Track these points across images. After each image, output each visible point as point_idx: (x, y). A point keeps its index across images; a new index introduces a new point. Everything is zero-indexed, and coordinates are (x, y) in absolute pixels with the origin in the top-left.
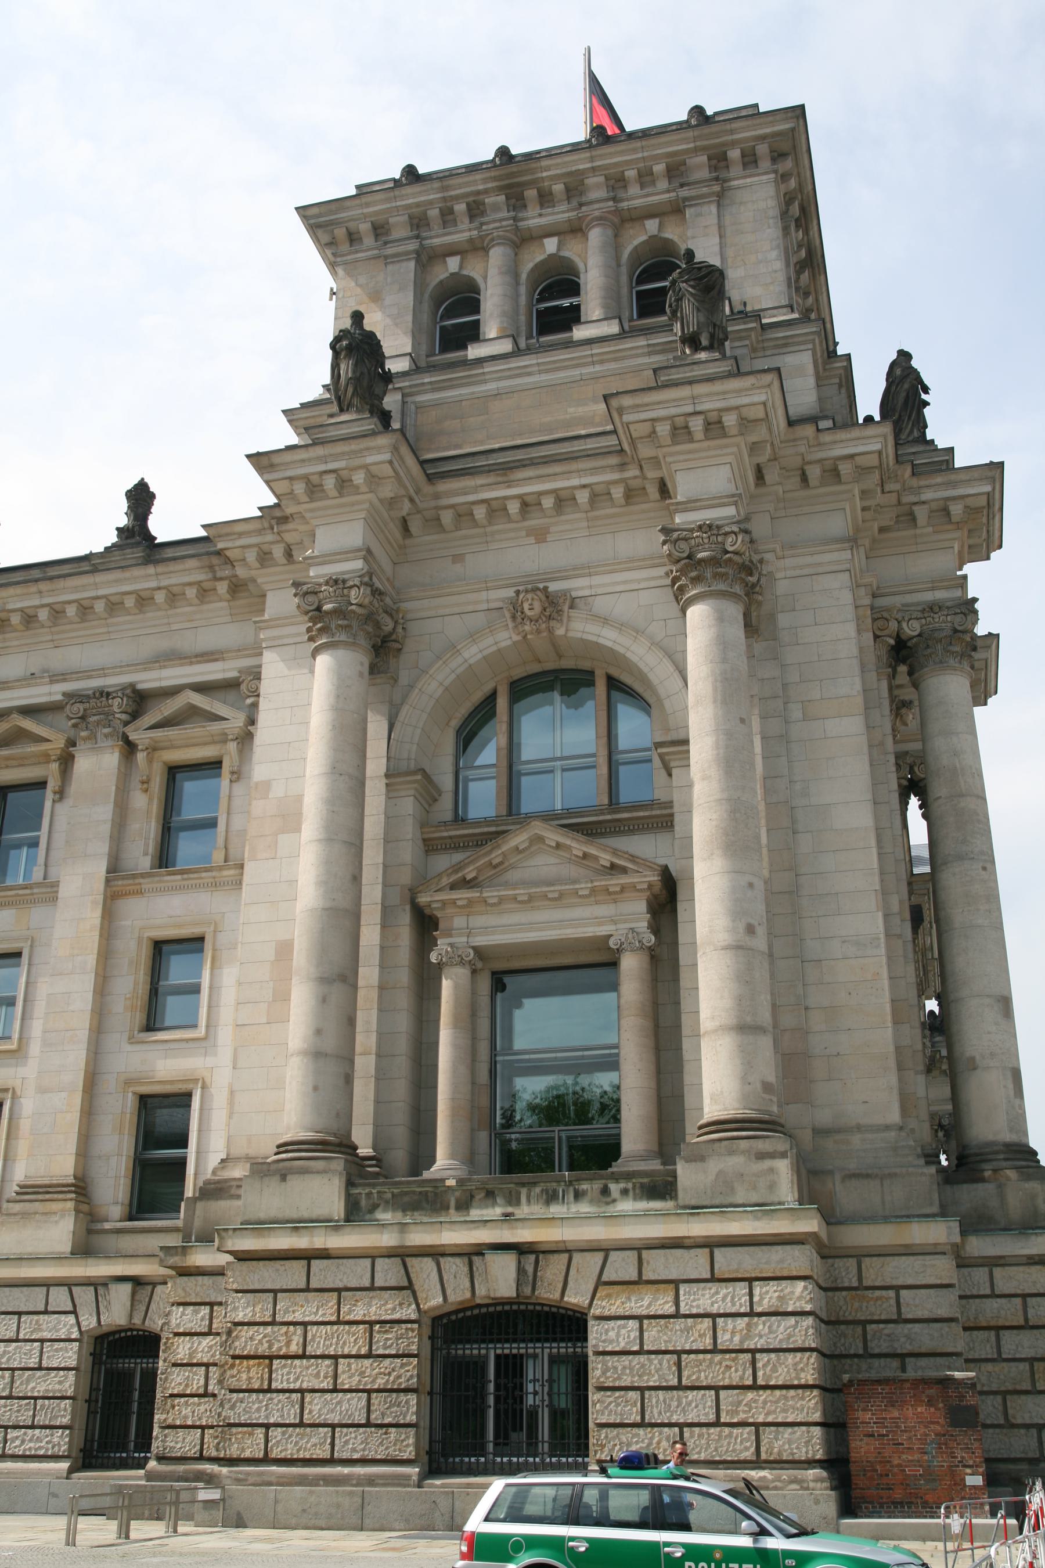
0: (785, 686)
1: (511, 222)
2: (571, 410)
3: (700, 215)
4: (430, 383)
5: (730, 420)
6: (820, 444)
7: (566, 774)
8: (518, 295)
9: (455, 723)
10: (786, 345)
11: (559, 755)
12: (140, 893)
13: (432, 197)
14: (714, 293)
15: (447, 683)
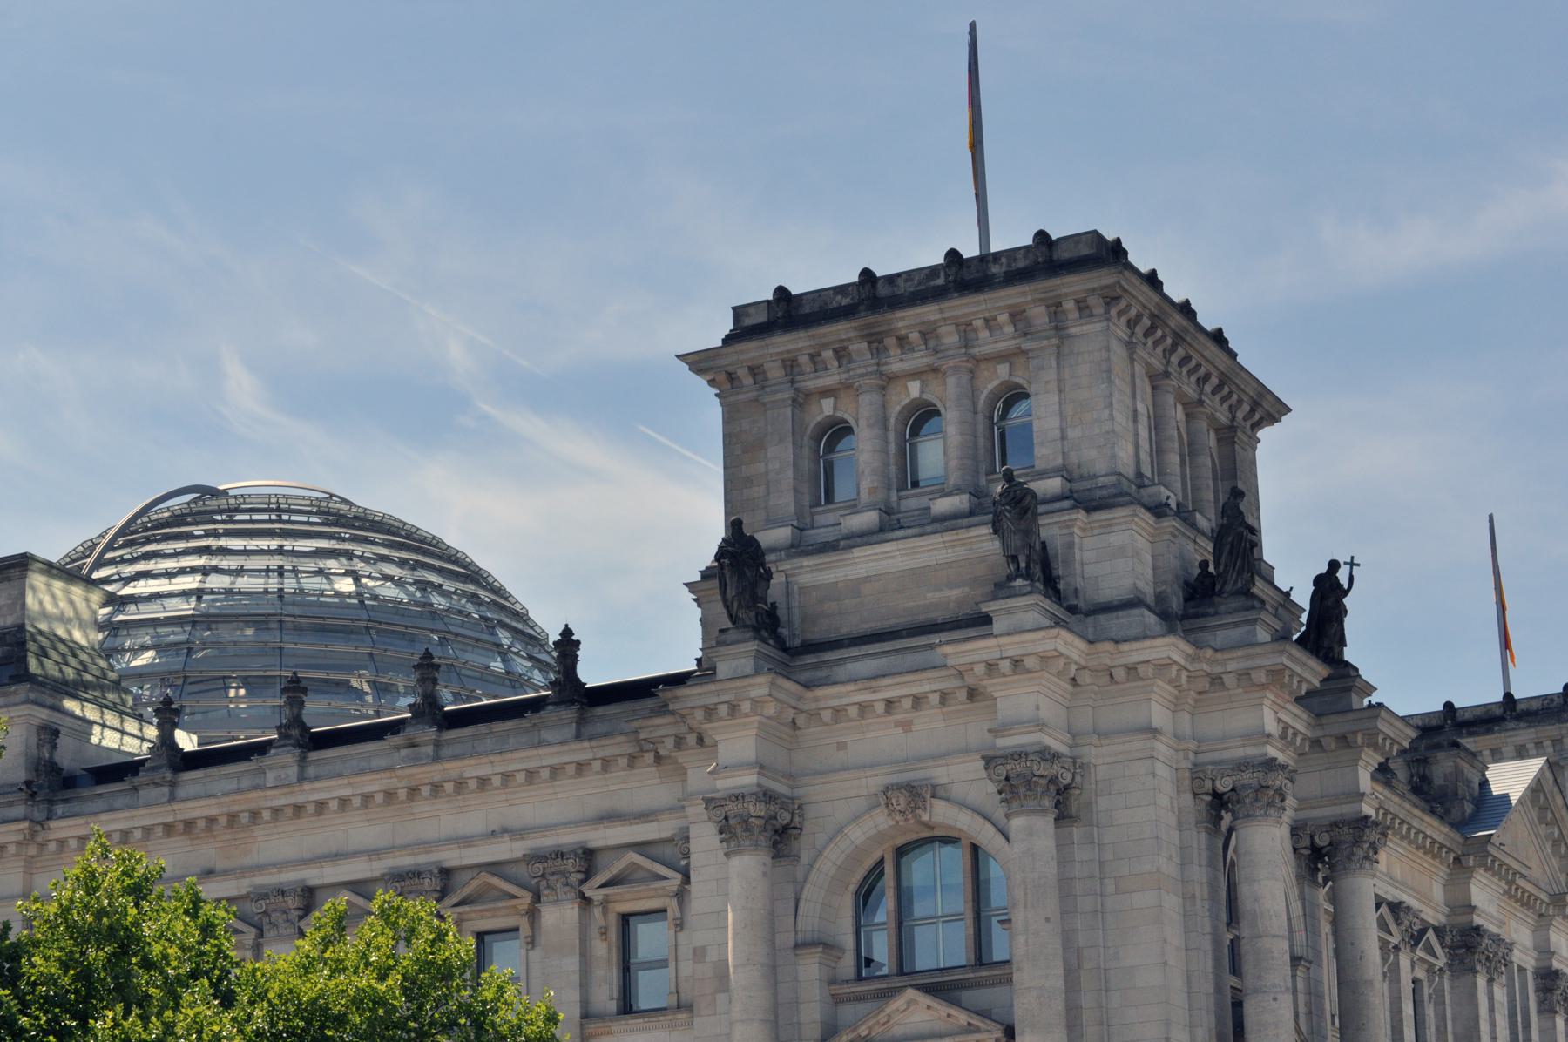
0: (1101, 863)
1: (876, 367)
2: (929, 595)
3: (1041, 368)
4: (809, 566)
5: (1030, 662)
6: (1120, 652)
7: (945, 925)
8: (887, 442)
9: (853, 888)
10: (1110, 525)
11: (940, 914)
12: (610, 1033)
13: (800, 345)
14: (1029, 514)
15: (838, 863)
